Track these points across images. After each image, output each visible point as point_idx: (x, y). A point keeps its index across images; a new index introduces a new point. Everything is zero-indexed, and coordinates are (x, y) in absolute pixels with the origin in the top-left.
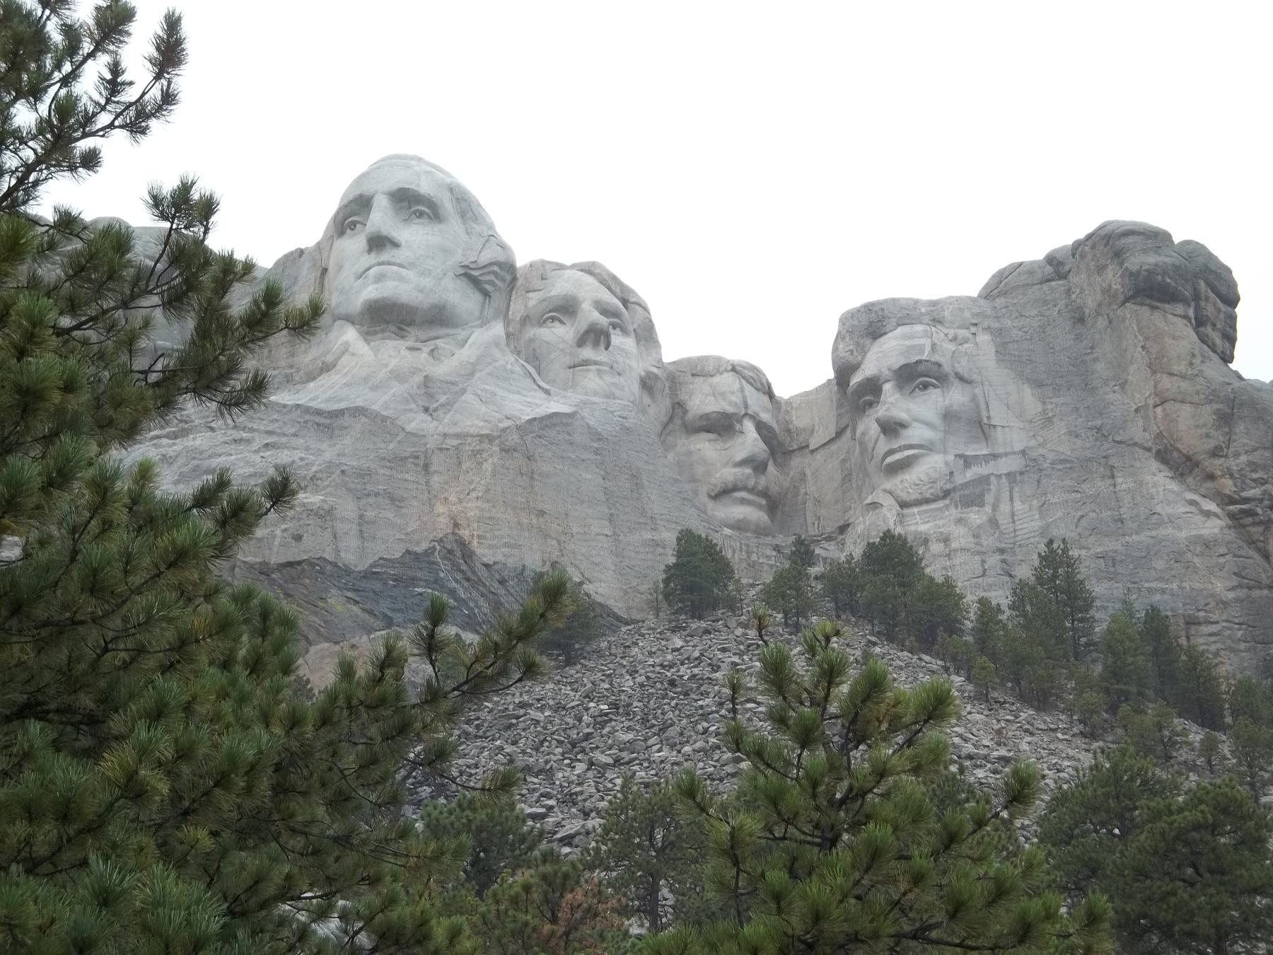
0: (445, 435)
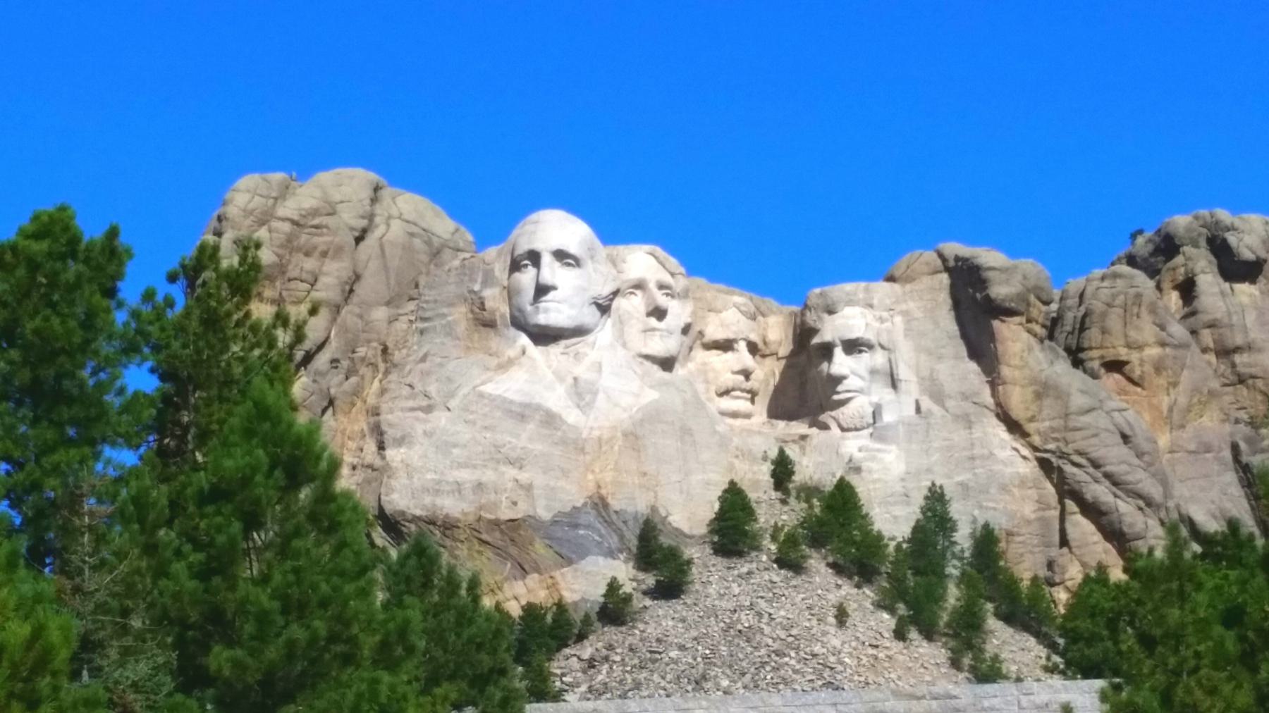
0: (592, 428)
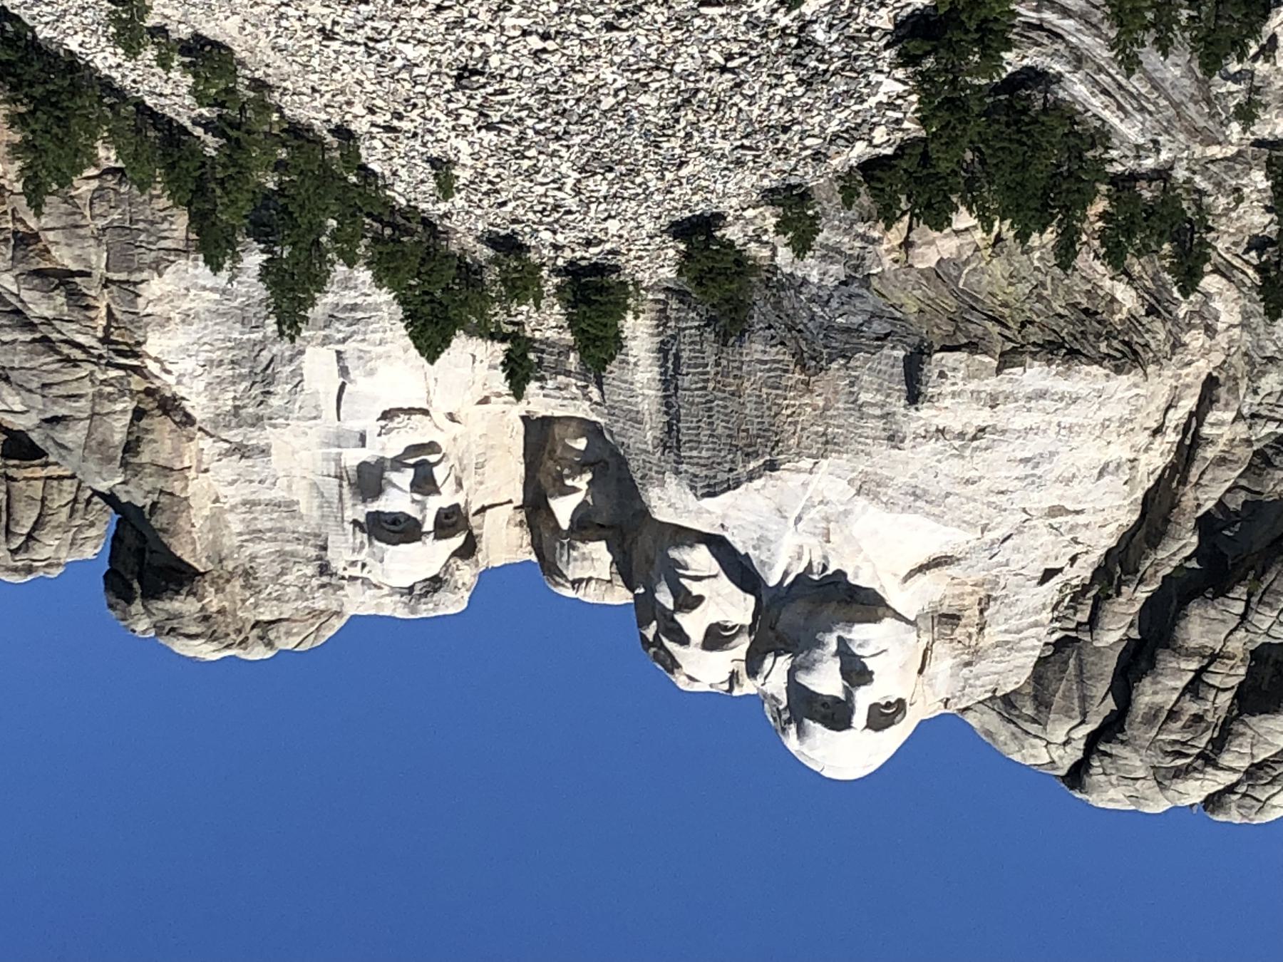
0: (811, 473)
